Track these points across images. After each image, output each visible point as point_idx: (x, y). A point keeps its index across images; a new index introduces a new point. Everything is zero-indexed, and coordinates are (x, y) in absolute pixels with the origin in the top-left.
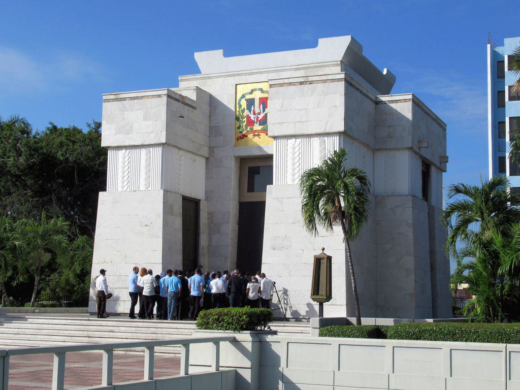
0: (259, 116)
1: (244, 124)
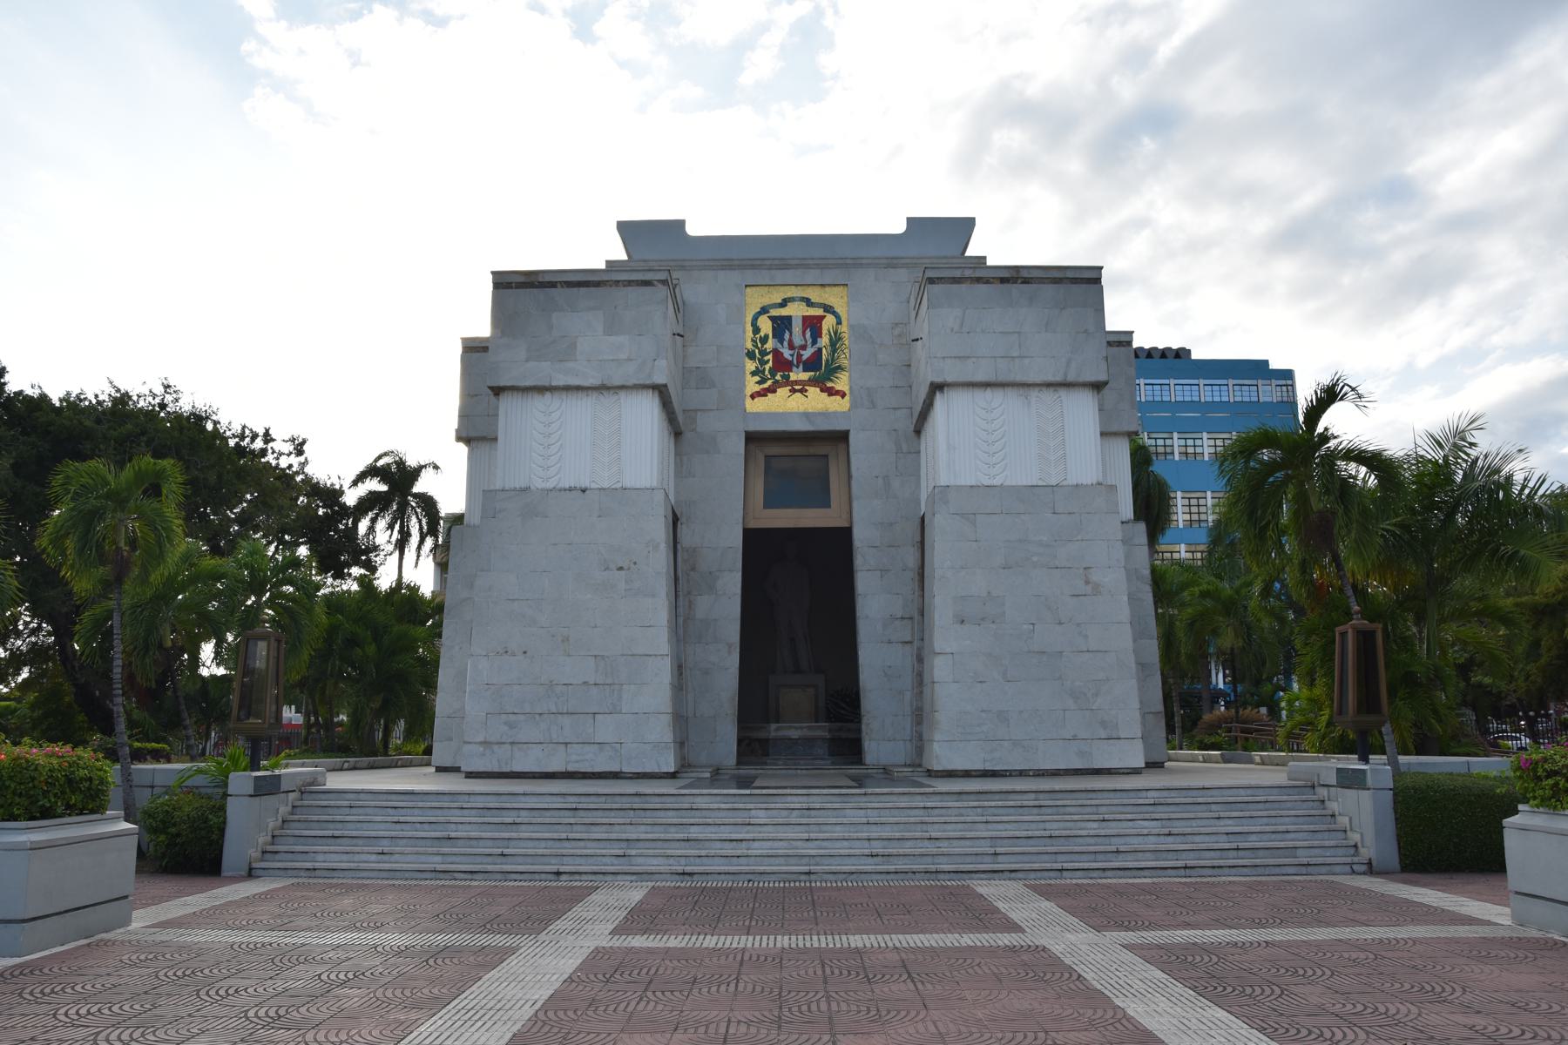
1: (767, 367)
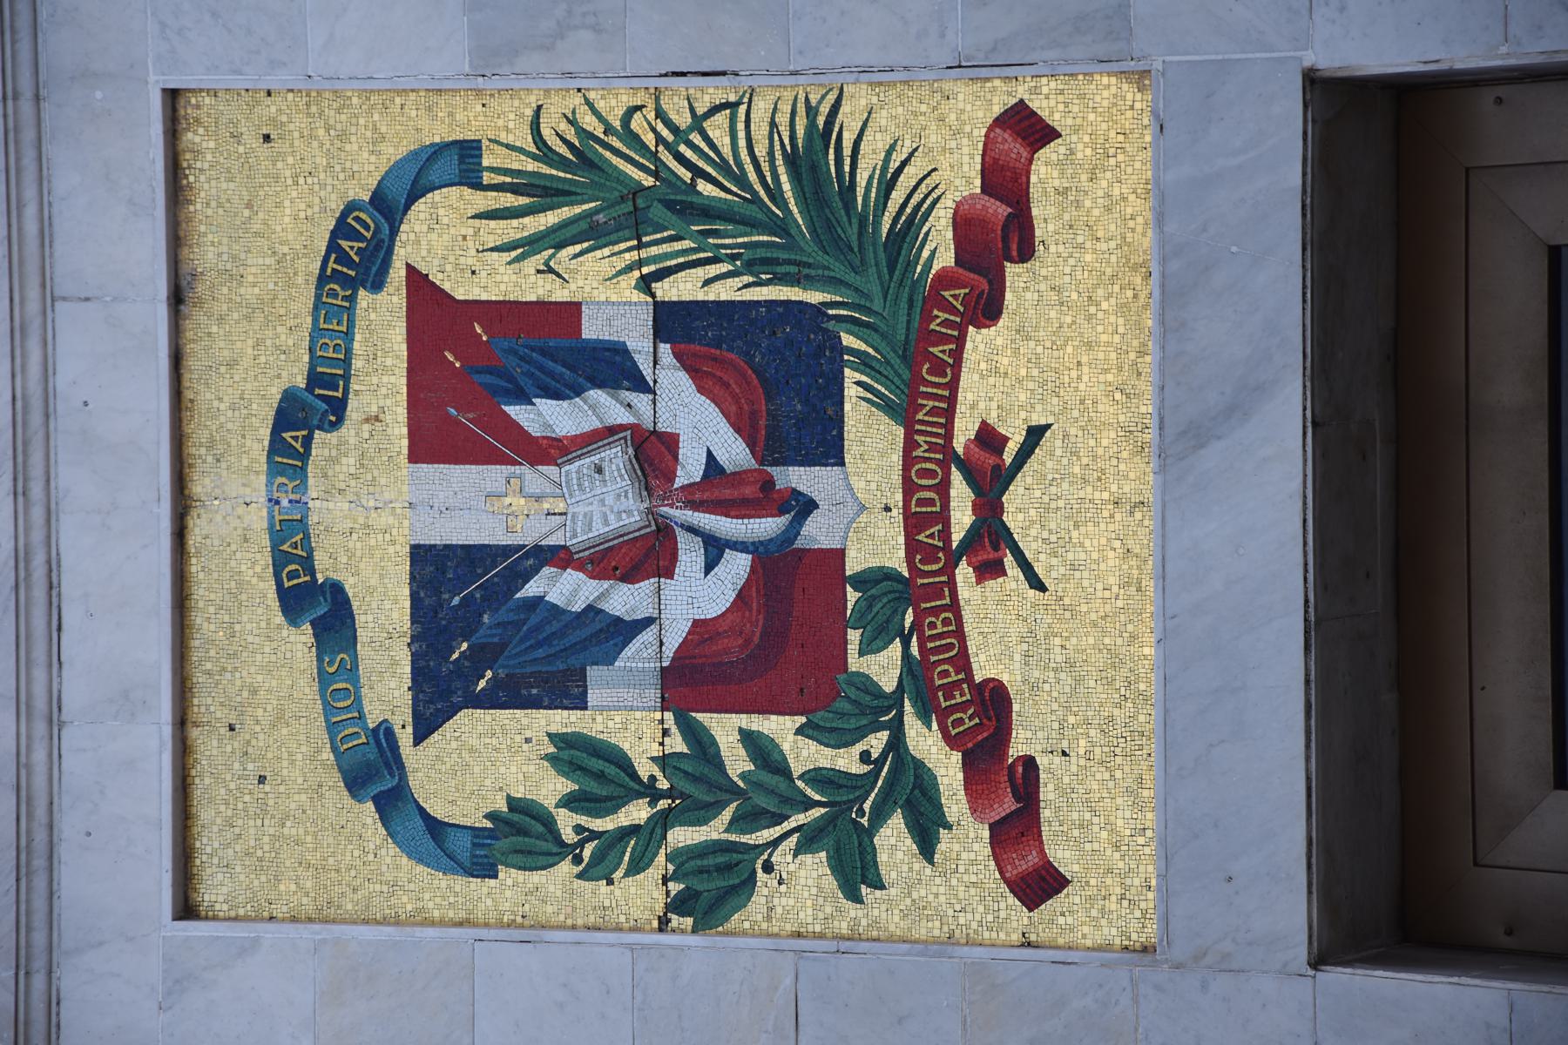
0: (690, 469)
1: (805, 755)
